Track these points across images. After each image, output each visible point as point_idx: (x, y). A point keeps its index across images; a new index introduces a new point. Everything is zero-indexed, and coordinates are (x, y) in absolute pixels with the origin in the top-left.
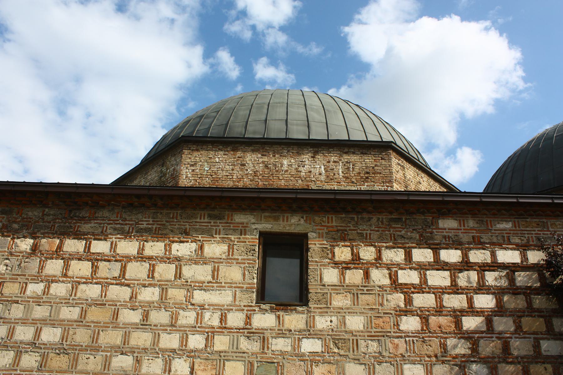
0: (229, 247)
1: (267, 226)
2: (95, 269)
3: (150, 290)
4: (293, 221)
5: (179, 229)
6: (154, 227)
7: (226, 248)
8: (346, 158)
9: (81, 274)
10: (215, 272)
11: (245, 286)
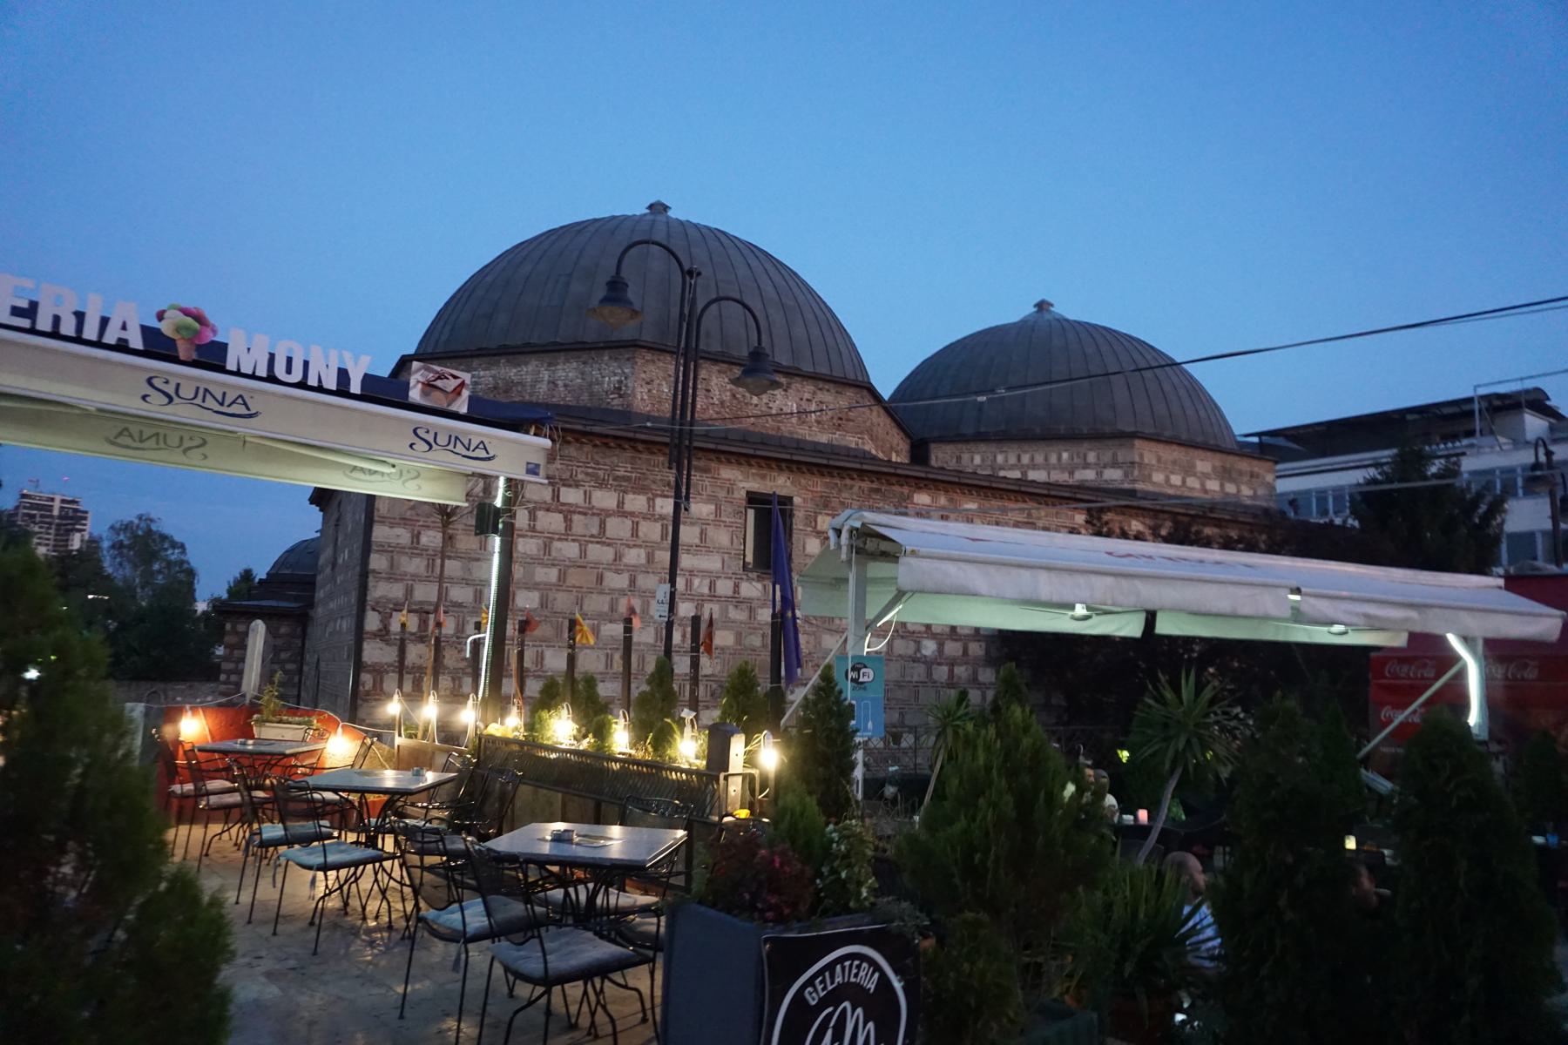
0: (716, 505)
1: (755, 485)
2: (568, 522)
3: (634, 552)
4: (780, 482)
5: (661, 480)
6: (634, 475)
7: (713, 507)
8: (820, 396)
9: (553, 528)
10: (703, 534)
11: (733, 552)
